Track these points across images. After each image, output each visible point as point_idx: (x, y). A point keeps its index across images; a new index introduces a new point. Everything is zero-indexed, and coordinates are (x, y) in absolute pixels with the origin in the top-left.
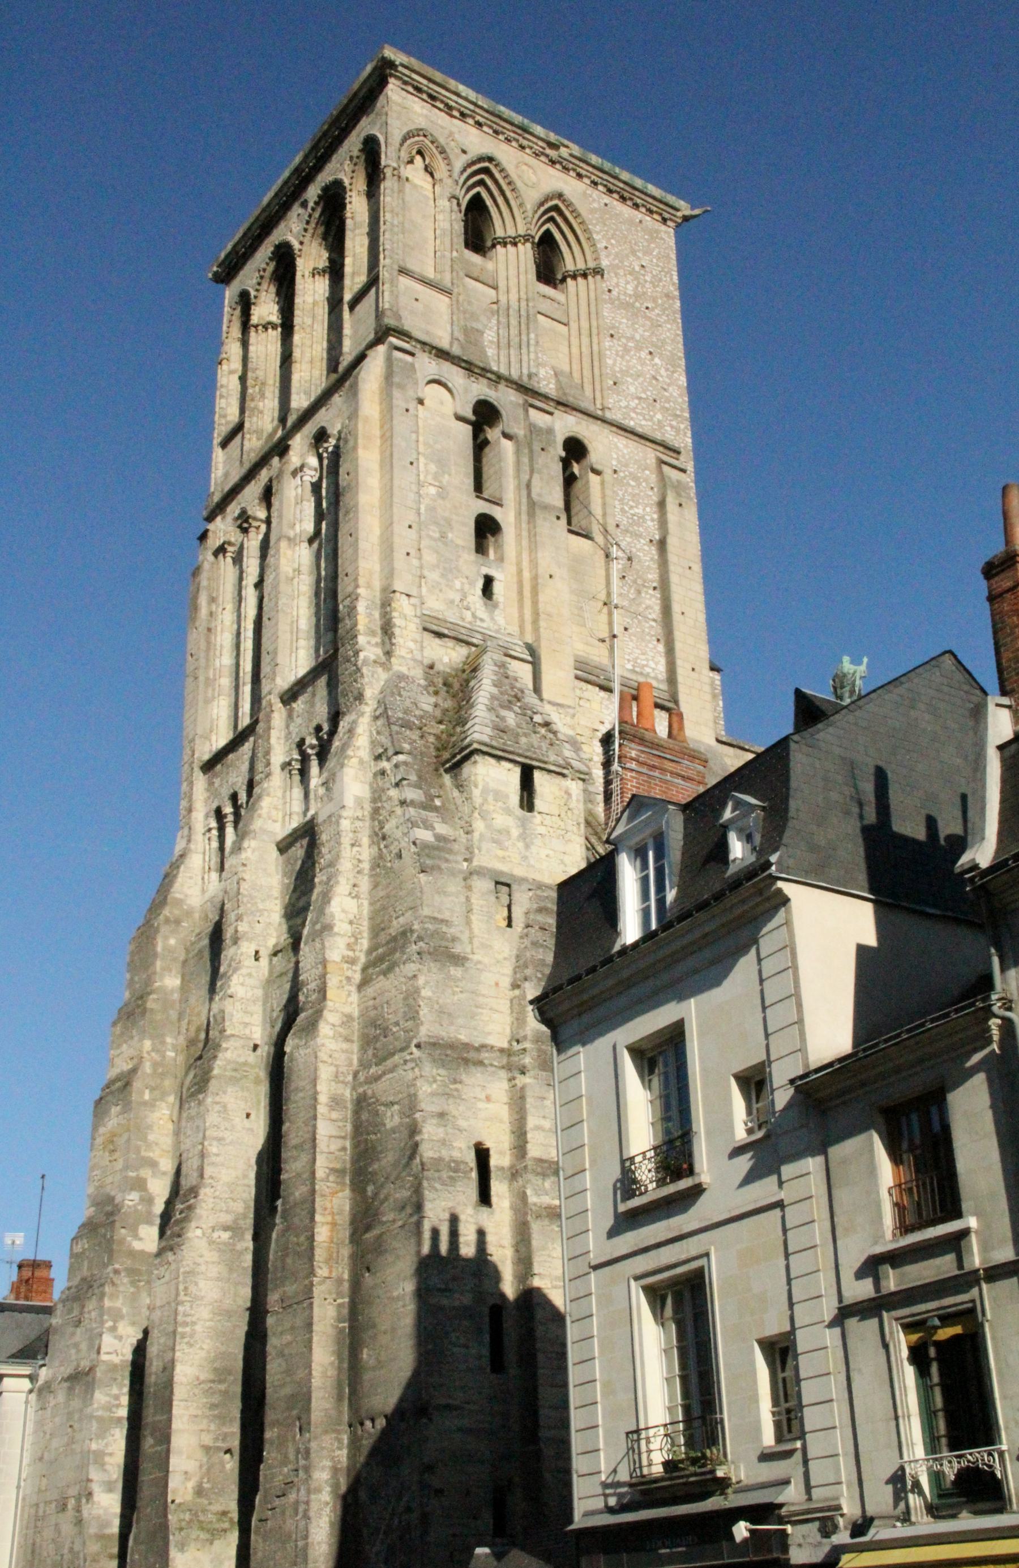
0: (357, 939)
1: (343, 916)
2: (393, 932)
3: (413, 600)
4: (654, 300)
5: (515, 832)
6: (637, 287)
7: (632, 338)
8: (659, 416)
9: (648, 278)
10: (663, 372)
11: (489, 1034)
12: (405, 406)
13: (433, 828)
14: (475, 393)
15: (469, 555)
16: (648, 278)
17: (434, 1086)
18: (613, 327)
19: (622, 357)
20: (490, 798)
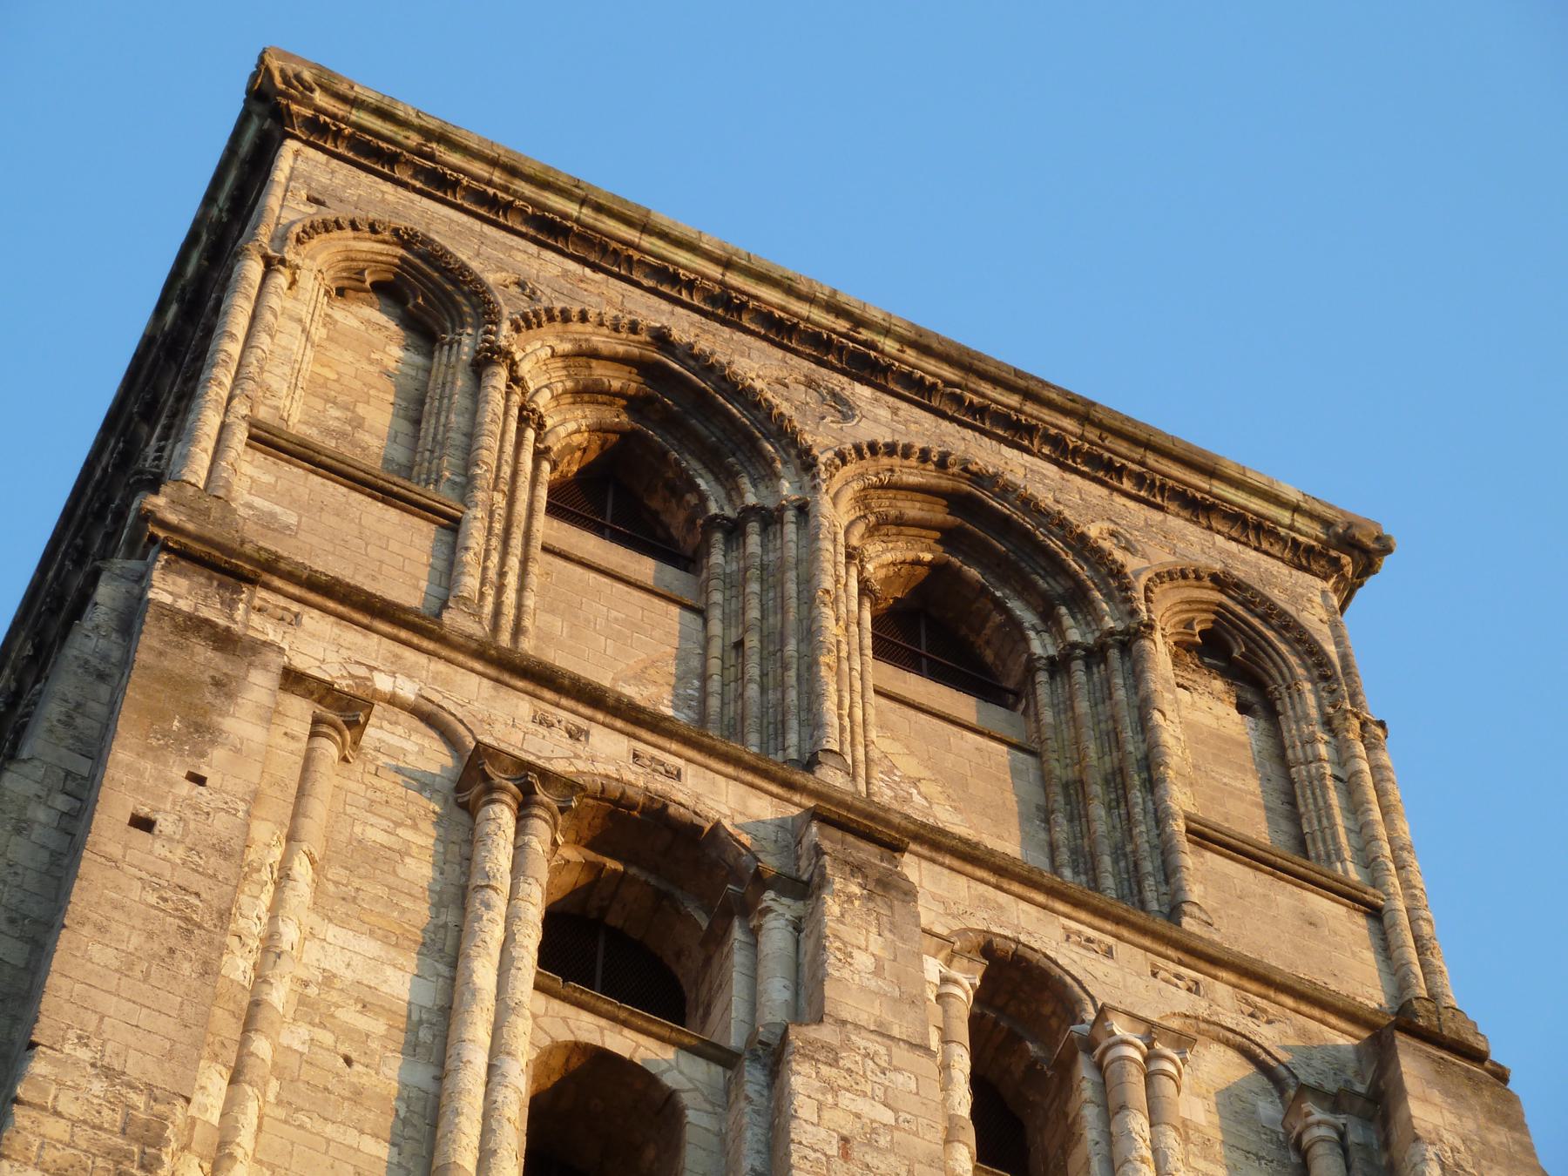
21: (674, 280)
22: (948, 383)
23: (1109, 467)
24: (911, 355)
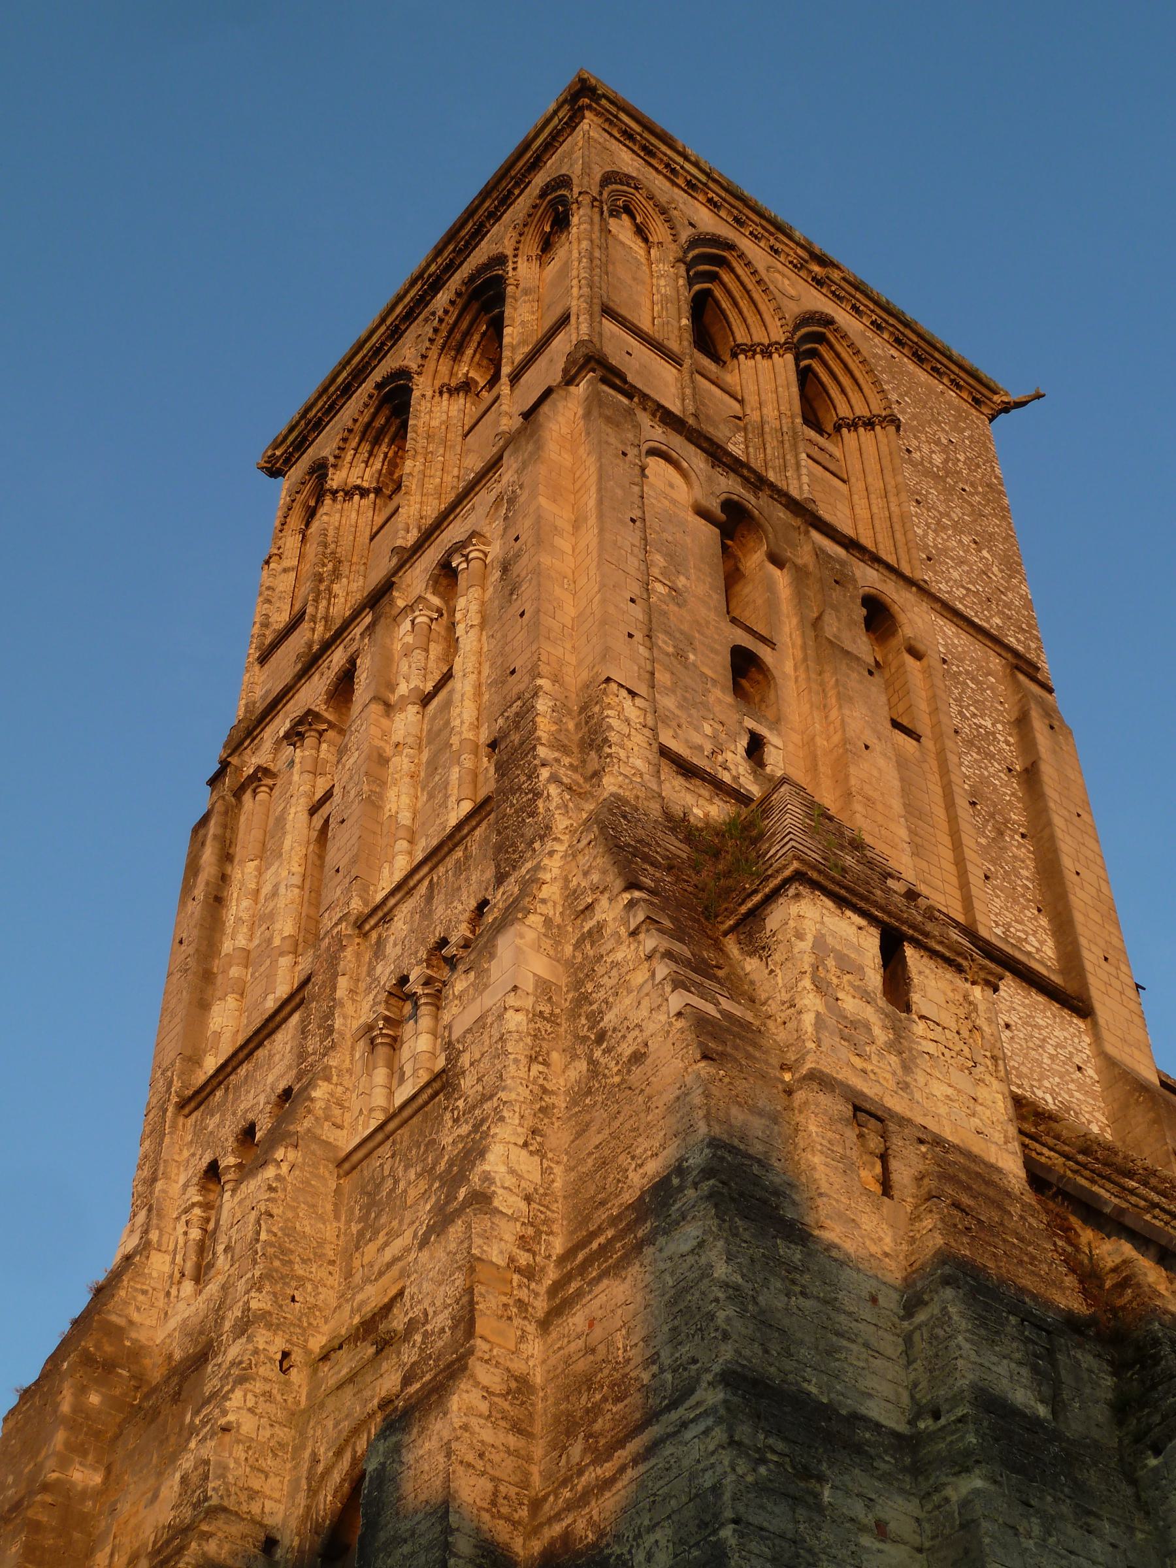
0: (539, 1233)
1: (510, 1181)
2: (628, 1197)
3: (638, 701)
4: (972, 485)
5: (881, 1035)
6: (946, 461)
7: (948, 515)
8: (997, 621)
9: (962, 458)
10: (995, 569)
11: (870, 1396)
12: (621, 447)
13: (717, 1004)
14: (724, 488)
15: (721, 697)
16: (962, 458)
17: (762, 1470)
18: (920, 494)
19: (935, 531)
20: (831, 963)
21: (379, 349)
22: (454, 251)
23: (507, 197)
24: (439, 260)
